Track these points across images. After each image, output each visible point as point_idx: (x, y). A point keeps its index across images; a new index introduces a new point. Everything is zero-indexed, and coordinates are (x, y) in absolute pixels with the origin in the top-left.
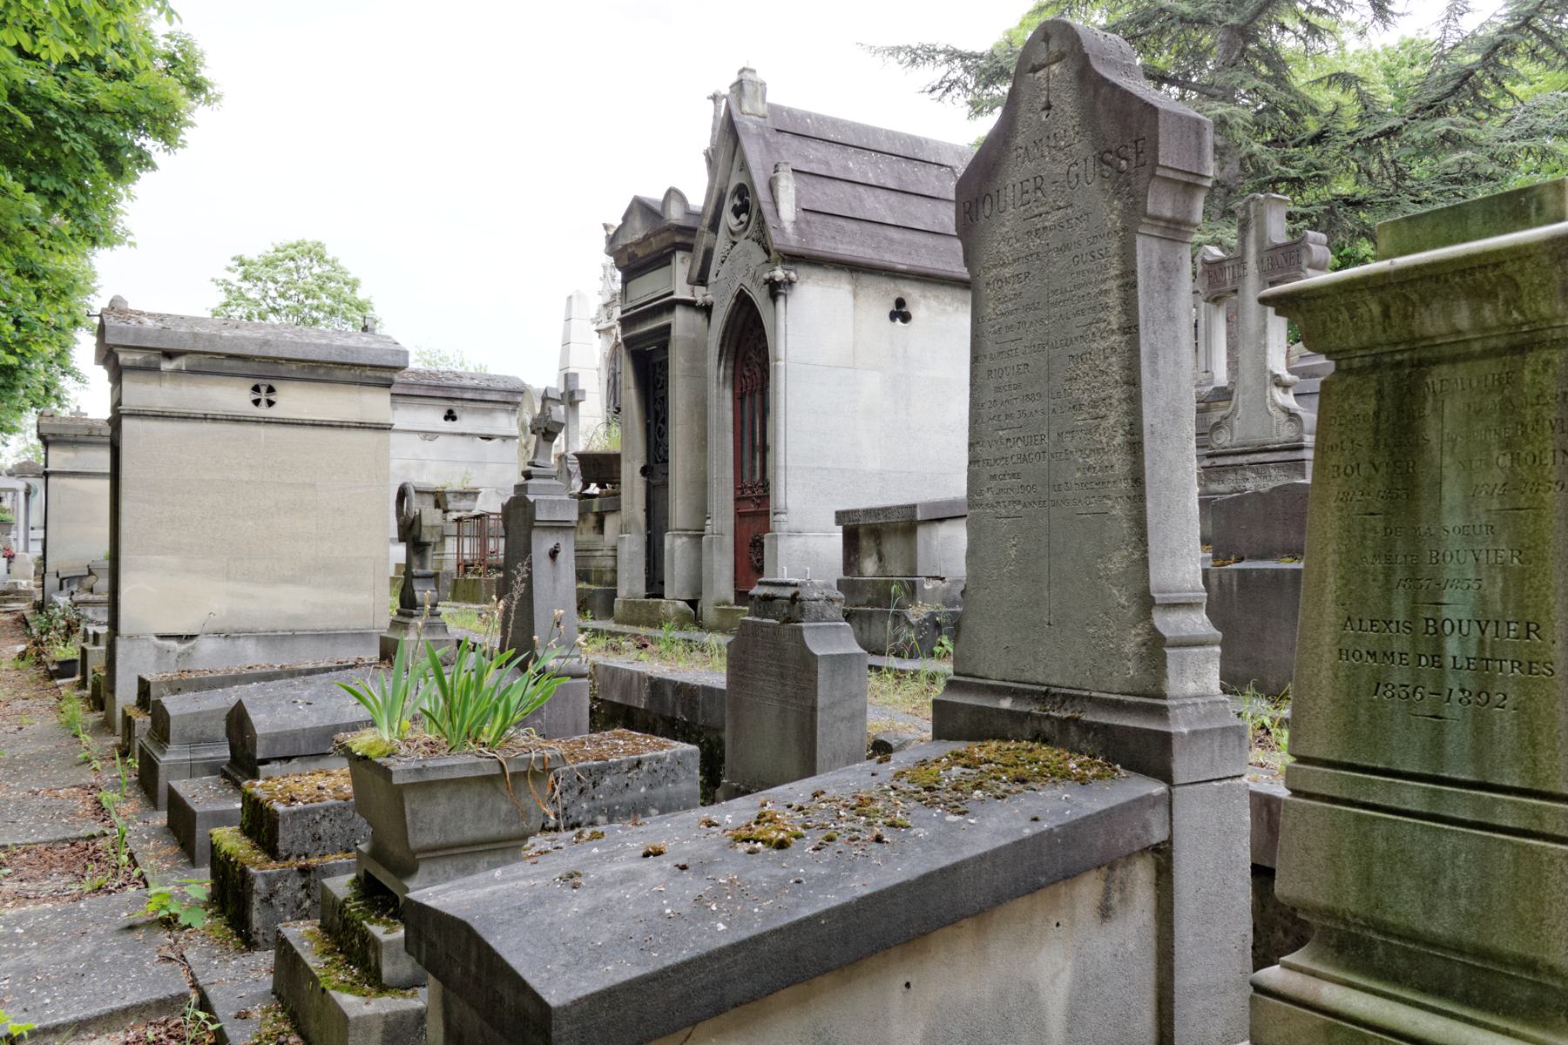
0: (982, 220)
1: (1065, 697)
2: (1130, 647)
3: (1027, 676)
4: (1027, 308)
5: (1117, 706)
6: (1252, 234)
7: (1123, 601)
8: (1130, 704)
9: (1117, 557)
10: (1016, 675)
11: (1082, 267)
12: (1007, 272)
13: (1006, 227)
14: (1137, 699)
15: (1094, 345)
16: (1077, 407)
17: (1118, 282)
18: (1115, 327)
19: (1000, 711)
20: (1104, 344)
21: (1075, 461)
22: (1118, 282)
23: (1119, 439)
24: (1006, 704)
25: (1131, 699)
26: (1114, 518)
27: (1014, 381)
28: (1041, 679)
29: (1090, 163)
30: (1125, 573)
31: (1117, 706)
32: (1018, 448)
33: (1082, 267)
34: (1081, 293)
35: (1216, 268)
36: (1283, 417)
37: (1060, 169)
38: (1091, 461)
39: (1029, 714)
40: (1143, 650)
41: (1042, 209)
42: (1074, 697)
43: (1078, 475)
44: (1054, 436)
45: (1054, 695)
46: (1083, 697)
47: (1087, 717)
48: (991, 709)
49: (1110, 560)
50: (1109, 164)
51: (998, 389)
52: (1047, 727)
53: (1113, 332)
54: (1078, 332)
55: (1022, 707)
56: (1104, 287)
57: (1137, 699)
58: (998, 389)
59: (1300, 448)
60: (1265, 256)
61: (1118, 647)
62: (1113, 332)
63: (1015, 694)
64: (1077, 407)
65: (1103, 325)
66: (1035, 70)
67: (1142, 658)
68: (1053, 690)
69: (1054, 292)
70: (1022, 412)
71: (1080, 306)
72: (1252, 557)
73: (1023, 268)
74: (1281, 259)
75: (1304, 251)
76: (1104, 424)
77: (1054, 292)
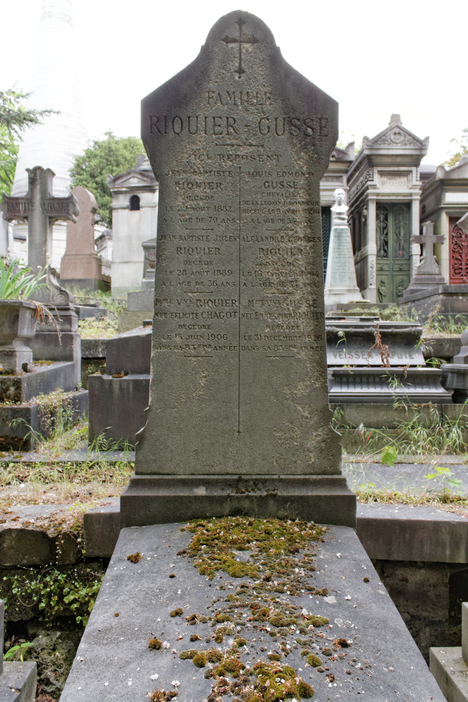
0: (171, 135)
1: (256, 482)
2: (311, 443)
3: (217, 469)
4: (219, 208)
5: (305, 483)
6: (38, 188)
7: (306, 414)
8: (315, 480)
9: (301, 386)
10: (207, 469)
11: (271, 190)
12: (198, 178)
13: (195, 148)
14: (320, 477)
15: (282, 245)
16: (267, 284)
17: (306, 207)
18: (302, 235)
19: (198, 498)
20: (290, 245)
21: (265, 321)
22: (306, 207)
23: (304, 309)
24: (201, 491)
25: (314, 477)
26: (299, 361)
27: (205, 258)
28: (230, 470)
29: (280, 122)
30: (309, 396)
31: (305, 483)
32: (208, 307)
33: (271, 190)
34: (271, 207)
35: (14, 202)
36: (57, 292)
37: (253, 118)
38: (279, 321)
39: (229, 496)
40: (323, 445)
41: (234, 142)
42: (265, 481)
43: (267, 330)
44: (244, 302)
45: (247, 481)
46: (273, 480)
47: (280, 493)
48: (189, 497)
49: (296, 387)
50: (296, 126)
51: (187, 262)
52: (246, 504)
53: (300, 239)
54: (268, 234)
55: (217, 493)
56: (292, 208)
57: (320, 477)
58: (187, 262)
59: (68, 309)
60: (47, 202)
61: (302, 444)
62: (300, 239)
63: (207, 483)
64: (267, 284)
65: (290, 233)
66: (228, 40)
67: (321, 451)
68: (246, 477)
69: (247, 202)
70: (213, 283)
71: (271, 216)
72: (133, 372)
73: (215, 179)
74: (56, 206)
75: (71, 205)
76: (291, 298)
77: (247, 202)
